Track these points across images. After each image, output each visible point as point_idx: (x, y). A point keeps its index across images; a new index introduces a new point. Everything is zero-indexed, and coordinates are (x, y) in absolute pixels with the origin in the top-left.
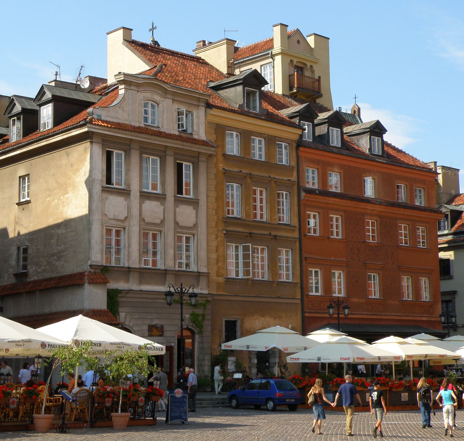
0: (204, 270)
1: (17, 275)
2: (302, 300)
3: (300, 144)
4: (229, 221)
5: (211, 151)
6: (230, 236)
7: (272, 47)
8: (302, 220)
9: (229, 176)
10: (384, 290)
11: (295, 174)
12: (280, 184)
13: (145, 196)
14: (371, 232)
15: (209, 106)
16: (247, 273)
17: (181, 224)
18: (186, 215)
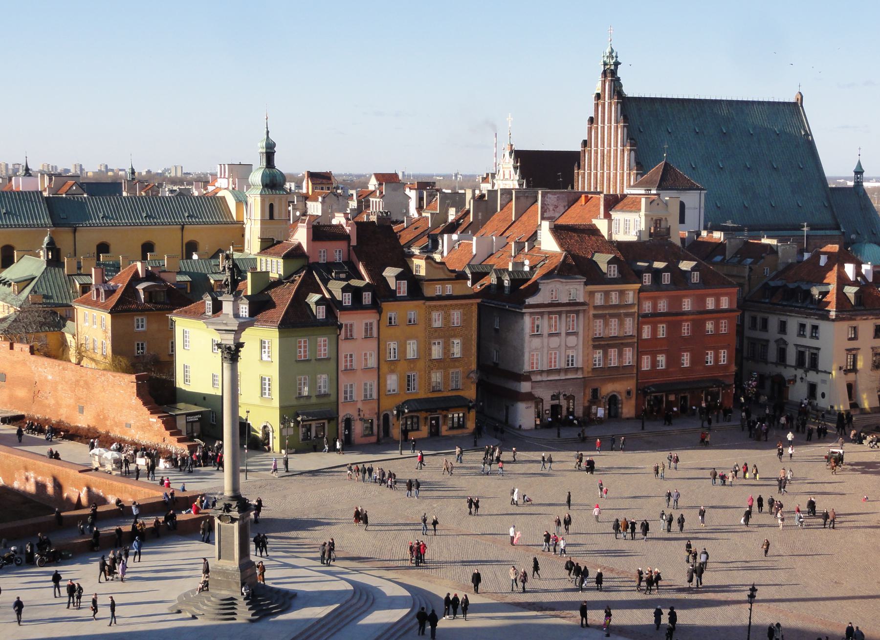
0: (580, 366)
1: (494, 363)
2: (637, 374)
3: (641, 290)
4: (595, 339)
5: (585, 308)
6: (595, 347)
7: (640, 210)
8: (639, 331)
9: (596, 316)
10: (693, 361)
11: (636, 307)
12: (627, 315)
13: (551, 335)
14: (686, 330)
15: (586, 284)
16: (605, 363)
17: (569, 345)
18: (572, 340)
